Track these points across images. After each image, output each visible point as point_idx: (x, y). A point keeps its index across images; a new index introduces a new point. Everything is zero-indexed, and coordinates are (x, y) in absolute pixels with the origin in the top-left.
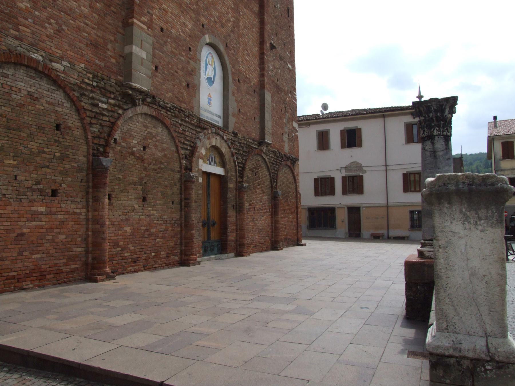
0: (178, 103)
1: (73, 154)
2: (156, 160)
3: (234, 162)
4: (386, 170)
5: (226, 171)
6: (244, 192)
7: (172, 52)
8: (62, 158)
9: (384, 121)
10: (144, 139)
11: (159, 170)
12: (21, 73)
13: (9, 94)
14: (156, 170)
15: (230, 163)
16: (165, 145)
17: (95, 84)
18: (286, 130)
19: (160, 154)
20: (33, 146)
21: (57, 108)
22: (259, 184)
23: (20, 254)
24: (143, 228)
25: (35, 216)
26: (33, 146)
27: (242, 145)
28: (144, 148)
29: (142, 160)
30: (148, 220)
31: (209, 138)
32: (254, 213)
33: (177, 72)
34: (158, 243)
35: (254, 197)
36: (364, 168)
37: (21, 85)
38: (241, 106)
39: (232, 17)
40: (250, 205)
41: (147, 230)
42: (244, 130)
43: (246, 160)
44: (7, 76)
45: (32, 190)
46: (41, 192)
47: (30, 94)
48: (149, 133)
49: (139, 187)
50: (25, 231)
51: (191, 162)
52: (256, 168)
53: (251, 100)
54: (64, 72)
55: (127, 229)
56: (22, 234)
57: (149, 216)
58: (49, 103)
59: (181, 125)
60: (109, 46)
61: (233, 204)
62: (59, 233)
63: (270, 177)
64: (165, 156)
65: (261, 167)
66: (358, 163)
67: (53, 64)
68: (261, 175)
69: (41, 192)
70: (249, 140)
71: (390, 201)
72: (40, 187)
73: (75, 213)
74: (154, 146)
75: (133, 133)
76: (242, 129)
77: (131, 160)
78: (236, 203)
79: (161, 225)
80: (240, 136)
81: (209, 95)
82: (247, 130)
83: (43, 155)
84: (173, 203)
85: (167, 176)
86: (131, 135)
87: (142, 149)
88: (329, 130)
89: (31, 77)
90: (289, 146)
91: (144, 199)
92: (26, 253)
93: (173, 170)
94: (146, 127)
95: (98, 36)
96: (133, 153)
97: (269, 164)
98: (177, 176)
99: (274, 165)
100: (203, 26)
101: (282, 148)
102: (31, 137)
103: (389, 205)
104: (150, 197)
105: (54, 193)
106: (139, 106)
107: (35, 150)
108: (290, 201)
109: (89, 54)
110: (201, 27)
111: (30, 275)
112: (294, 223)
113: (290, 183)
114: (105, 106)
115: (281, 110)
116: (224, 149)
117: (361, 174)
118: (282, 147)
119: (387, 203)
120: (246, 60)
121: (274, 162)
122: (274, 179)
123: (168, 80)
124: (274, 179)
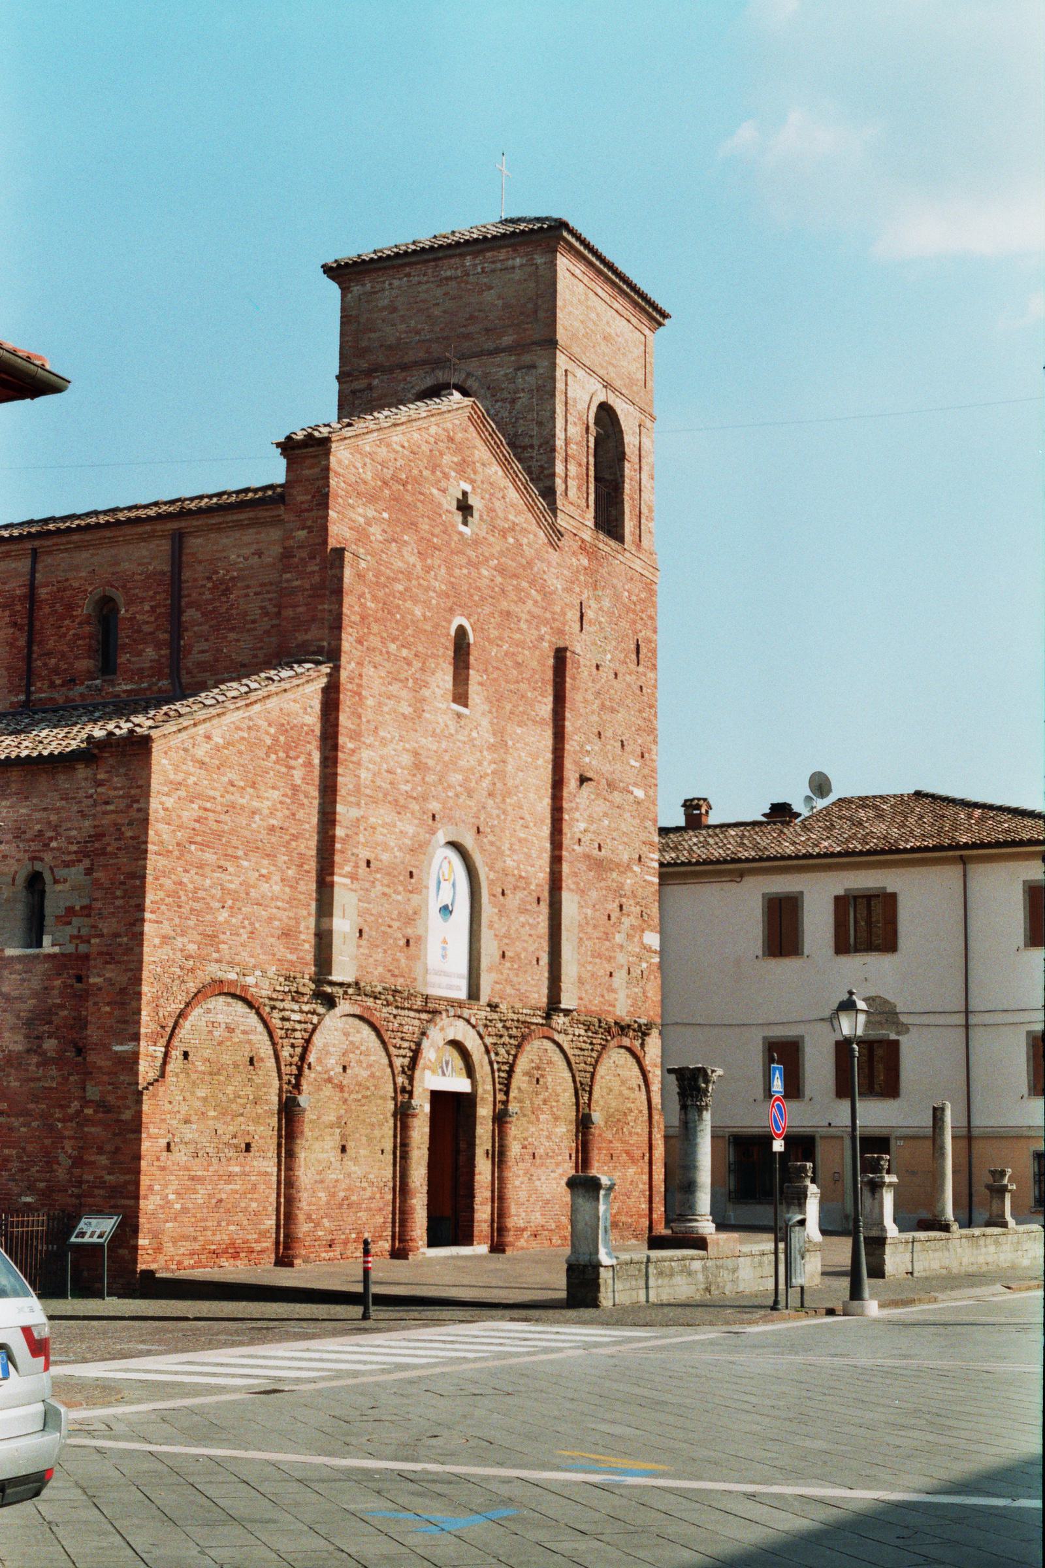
0: (392, 980)
3: (491, 1063)
4: (967, 1026)
5: (474, 1084)
6: (510, 1123)
9: (965, 875)
10: (344, 1055)
11: (363, 1101)
14: (359, 1100)
16: (373, 1058)
18: (621, 958)
21: (251, 1037)
22: (545, 1102)
24: (342, 1194)
27: (508, 1024)
28: (345, 1068)
29: (341, 1088)
32: (533, 1164)
33: (390, 926)
35: (533, 1129)
36: (904, 1019)
37: (220, 1018)
40: (524, 1147)
41: (346, 1198)
42: (513, 992)
43: (515, 1056)
44: (209, 1011)
48: (352, 1043)
49: (338, 1131)
50: (224, 1196)
51: (411, 1079)
52: (538, 1068)
54: (256, 985)
55: (321, 1194)
56: (220, 1201)
57: (349, 1175)
58: (244, 1032)
59: (395, 1016)
63: (574, 1081)
64: (372, 1076)
65: (550, 1062)
66: (886, 1002)
70: (525, 1011)
71: (976, 1121)
72: (235, 1141)
76: (509, 990)
78: (493, 1146)
79: (364, 1189)
80: (503, 1007)
81: (445, 942)
82: (518, 990)
83: (239, 1100)
86: (328, 1053)
88: (802, 893)
90: (628, 996)
91: (343, 1149)
92: (223, 1224)
93: (383, 1098)
95: (290, 918)
97: (570, 1052)
98: (391, 1106)
99: (586, 1053)
101: (610, 1009)
103: (975, 1132)
104: (350, 1145)
107: (231, 1096)
108: (630, 1133)
109: (281, 951)
111: (225, 1251)
112: (641, 1186)
113: (630, 1089)
115: (609, 917)
116: (473, 1044)
117: (893, 1037)
118: (610, 1005)
119: (969, 1127)
120: (520, 841)
121: (584, 1046)
122: (583, 1089)
124: (583, 1089)
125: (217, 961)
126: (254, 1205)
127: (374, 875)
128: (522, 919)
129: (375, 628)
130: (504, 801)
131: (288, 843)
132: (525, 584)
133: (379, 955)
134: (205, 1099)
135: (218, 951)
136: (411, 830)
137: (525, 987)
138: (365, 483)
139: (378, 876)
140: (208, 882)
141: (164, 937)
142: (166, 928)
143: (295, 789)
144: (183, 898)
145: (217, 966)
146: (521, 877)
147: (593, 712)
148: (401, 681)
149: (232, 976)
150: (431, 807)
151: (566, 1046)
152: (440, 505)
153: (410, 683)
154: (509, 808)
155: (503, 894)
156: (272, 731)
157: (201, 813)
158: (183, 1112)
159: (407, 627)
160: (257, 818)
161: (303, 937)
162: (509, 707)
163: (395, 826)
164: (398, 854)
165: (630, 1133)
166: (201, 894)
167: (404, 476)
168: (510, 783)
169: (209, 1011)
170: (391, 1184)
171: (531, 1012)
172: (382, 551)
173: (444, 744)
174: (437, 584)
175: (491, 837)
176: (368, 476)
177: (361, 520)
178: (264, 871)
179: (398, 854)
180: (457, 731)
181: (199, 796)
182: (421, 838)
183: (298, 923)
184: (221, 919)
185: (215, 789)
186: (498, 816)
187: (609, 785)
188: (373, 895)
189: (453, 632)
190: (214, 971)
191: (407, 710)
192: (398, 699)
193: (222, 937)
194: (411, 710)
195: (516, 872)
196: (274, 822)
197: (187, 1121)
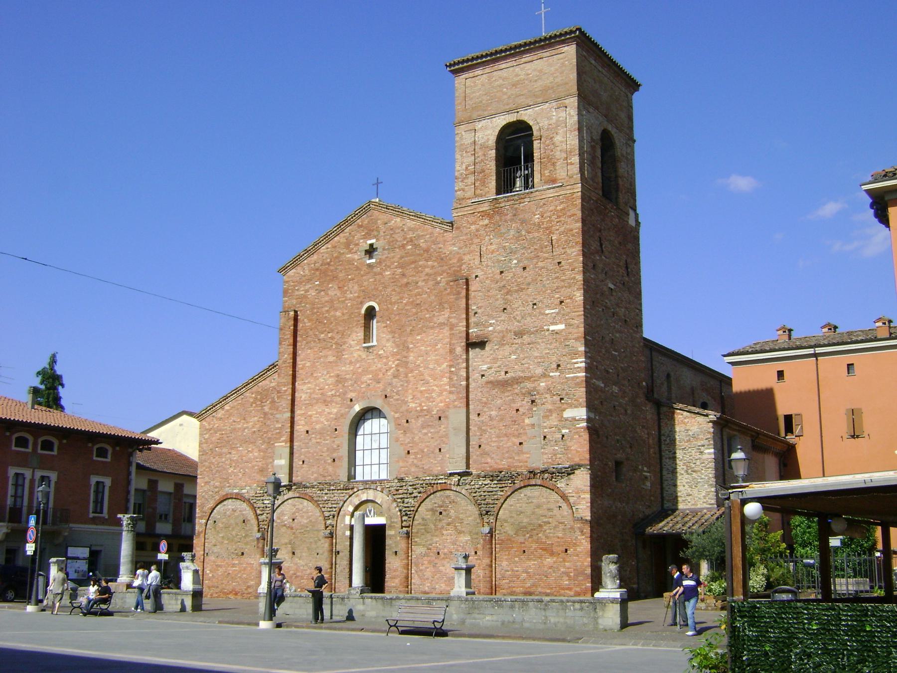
0: (323, 479)
1: (251, 533)
2: (302, 525)
7: (317, 442)
8: (245, 537)
10: (293, 514)
12: (230, 500)
13: (225, 513)
15: (390, 510)
16: (310, 514)
17: (262, 492)
19: (305, 521)
20: (234, 533)
23: (228, 582)
25: (234, 565)
26: (234, 533)
29: (292, 528)
30: (295, 567)
31: (357, 496)
34: (303, 582)
38: (410, 447)
39: (393, 362)
44: (224, 505)
45: (233, 553)
46: (237, 554)
47: (233, 510)
48: (297, 509)
49: (289, 546)
50: (230, 572)
53: (431, 433)
56: (229, 573)
57: (296, 564)
58: (240, 511)
60: (269, 466)
61: (394, 550)
62: (243, 574)
67: (243, 491)
68: (452, 511)
69: (237, 554)
73: (251, 564)
74: (301, 516)
75: (285, 512)
77: (283, 530)
80: (410, 478)
84: (318, 554)
85: (312, 536)
87: (291, 521)
89: (234, 502)
91: (294, 553)
94: (295, 506)
95: (263, 464)
96: (285, 525)
100: (351, 400)
102: (233, 529)
105: (243, 554)
106: (284, 495)
110: (349, 403)
111: (231, 592)
114: (268, 502)
120: (421, 392)
121: (491, 489)
123: (313, 466)
125: (229, 487)
126: (245, 576)
127: (311, 436)
128: (425, 431)
129: (311, 333)
130: (406, 376)
131: (262, 435)
132: (420, 263)
133: (314, 469)
134: (223, 537)
135: (229, 483)
136: (335, 410)
137: (428, 466)
138: (305, 276)
139: (313, 436)
140: (223, 459)
141: (206, 482)
142: (207, 479)
143: (265, 414)
144: (213, 467)
145: (229, 488)
146: (422, 410)
147: (497, 300)
148: (327, 348)
149: (236, 491)
150: (349, 396)
151: (463, 492)
152: (354, 260)
153: (334, 347)
154: (412, 379)
155: (407, 421)
156: (254, 396)
157: (221, 436)
158: (213, 542)
159: (332, 323)
160: (246, 430)
161: (270, 470)
162: (408, 330)
163: (324, 411)
164: (326, 423)
165: (547, 537)
166: (220, 464)
167: (329, 260)
168: (411, 366)
169: (224, 505)
170: (337, 566)
171: (435, 478)
172: (316, 299)
173: (358, 365)
174: (352, 295)
175: (397, 397)
176: (307, 272)
177: (303, 292)
178: (250, 449)
179: (326, 423)
180: (367, 356)
181: (220, 430)
182: (343, 412)
183: (267, 465)
184: (230, 471)
185: (226, 426)
186: (402, 385)
187: (516, 334)
188: (310, 444)
189: (363, 311)
190: (227, 490)
191: (331, 359)
192: (326, 356)
193: (230, 478)
194: (335, 358)
195: (418, 408)
196: (255, 429)
197: (215, 545)
